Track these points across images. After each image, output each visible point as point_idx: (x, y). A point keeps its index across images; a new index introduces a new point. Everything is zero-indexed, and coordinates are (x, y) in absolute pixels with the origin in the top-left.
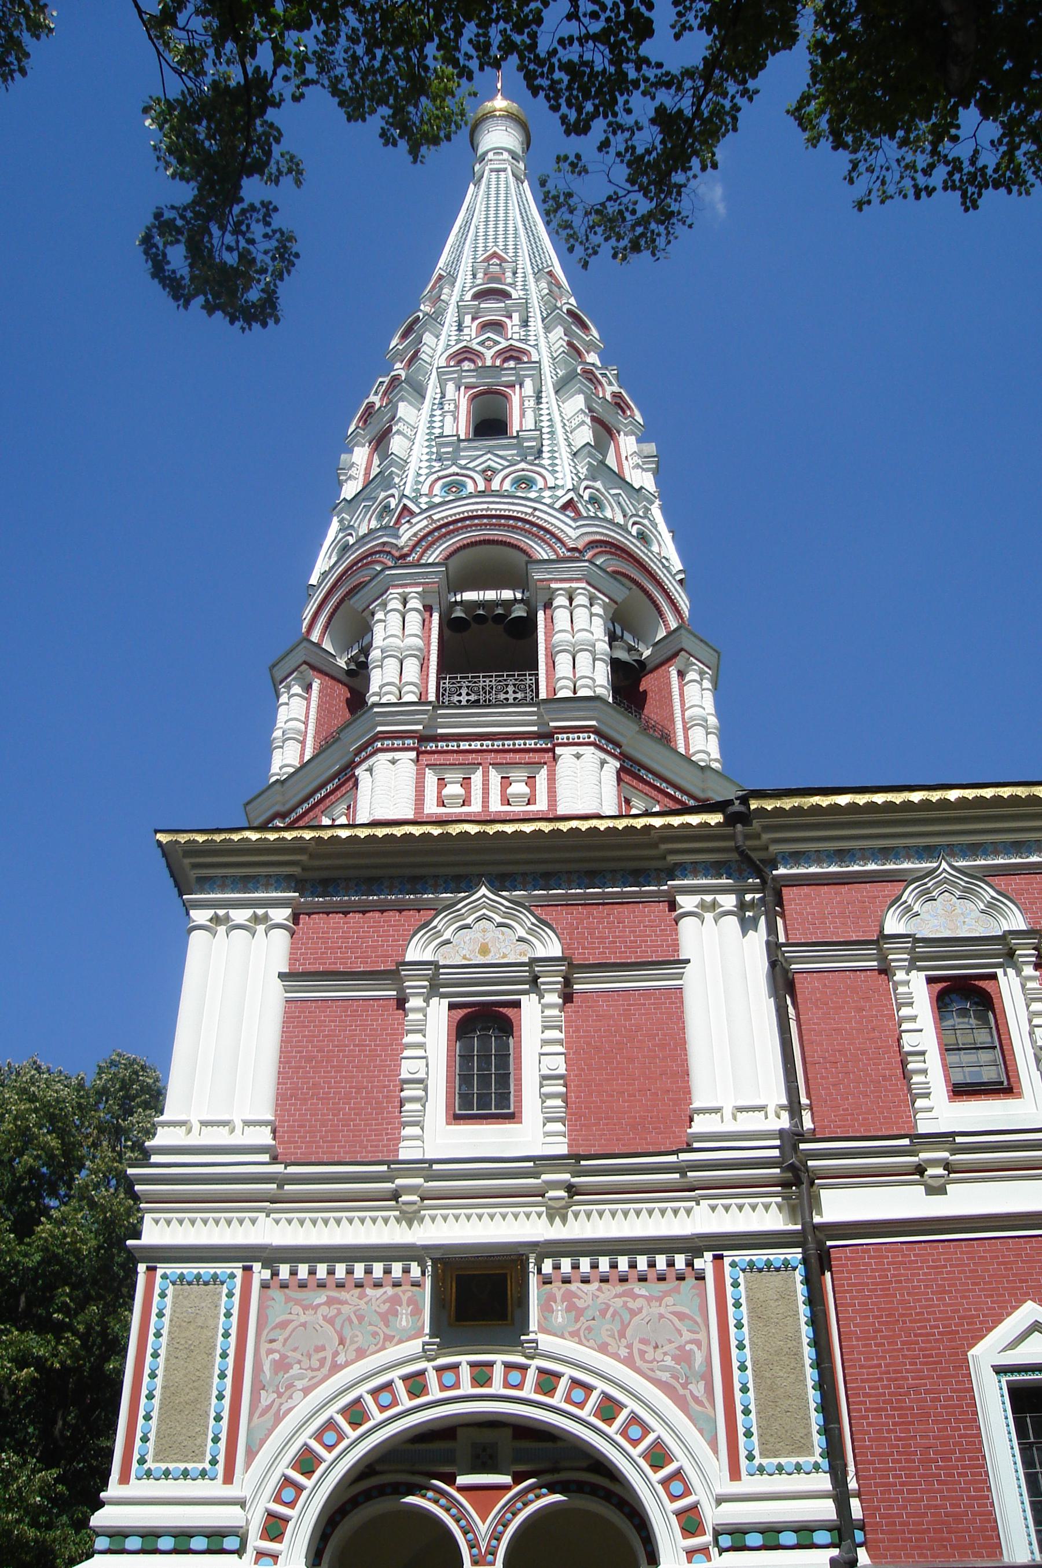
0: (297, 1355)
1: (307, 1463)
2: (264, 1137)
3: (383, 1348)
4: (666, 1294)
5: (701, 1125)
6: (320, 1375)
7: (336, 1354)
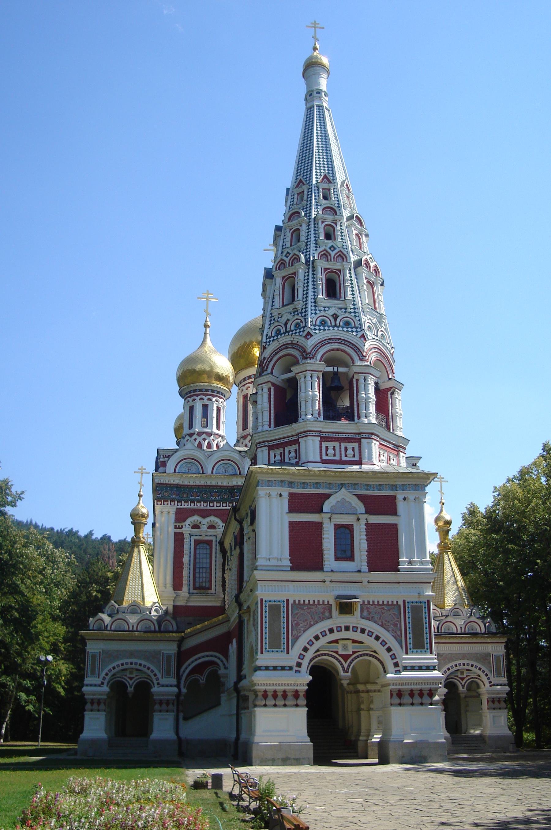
0: (301, 622)
1: (305, 649)
3: (322, 620)
4: (391, 609)
6: (307, 627)
7: (311, 622)
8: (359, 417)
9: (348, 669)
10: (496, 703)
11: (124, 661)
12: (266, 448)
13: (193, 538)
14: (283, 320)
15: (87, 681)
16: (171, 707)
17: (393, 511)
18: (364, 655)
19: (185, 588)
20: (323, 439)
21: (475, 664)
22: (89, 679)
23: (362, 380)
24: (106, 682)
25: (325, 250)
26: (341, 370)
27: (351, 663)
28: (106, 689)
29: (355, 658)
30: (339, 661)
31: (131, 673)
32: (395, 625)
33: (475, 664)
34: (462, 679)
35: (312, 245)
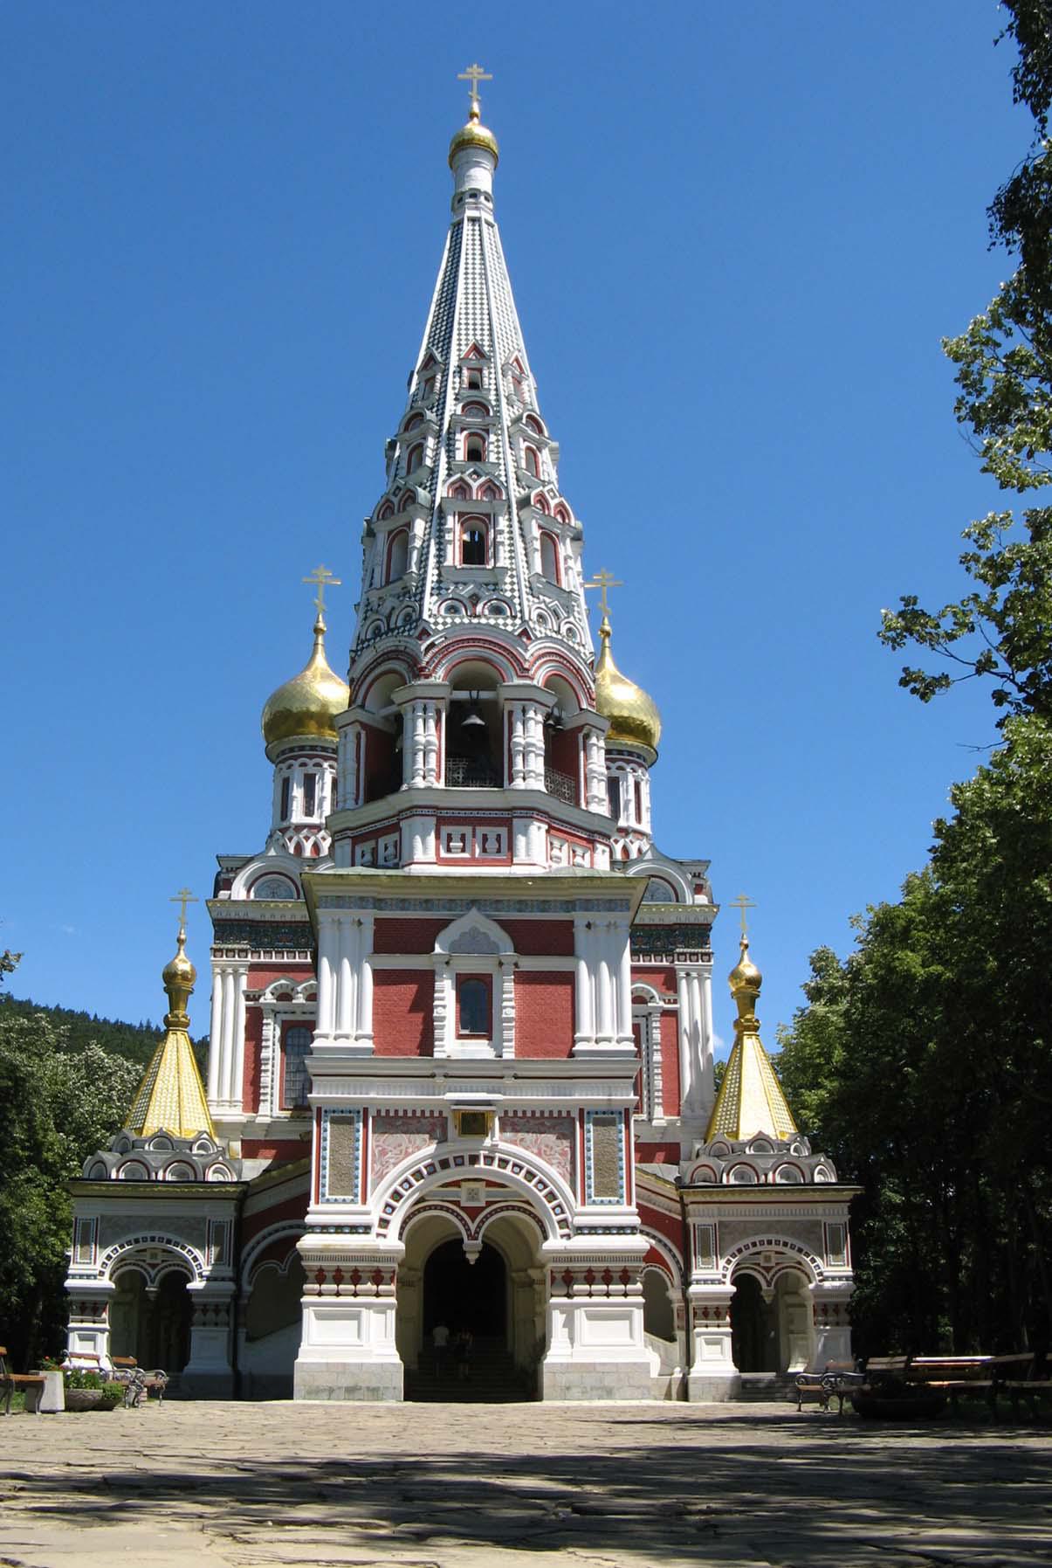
2: (369, 1044)
5: (579, 1047)
8: (511, 780)
9: (477, 1233)
10: (831, 1311)
12: (349, 841)
14: (385, 609)
15: (73, 1268)
16: (223, 1316)
17: (568, 950)
18: (507, 1208)
19: (264, 1108)
20: (441, 821)
21: (790, 1241)
23: (518, 714)
24: (108, 1271)
25: (461, 479)
26: (485, 695)
27: (482, 1222)
29: (491, 1214)
30: (462, 1219)
31: (154, 1256)
32: (563, 1154)
33: (790, 1241)
34: (768, 1269)
35: (443, 472)
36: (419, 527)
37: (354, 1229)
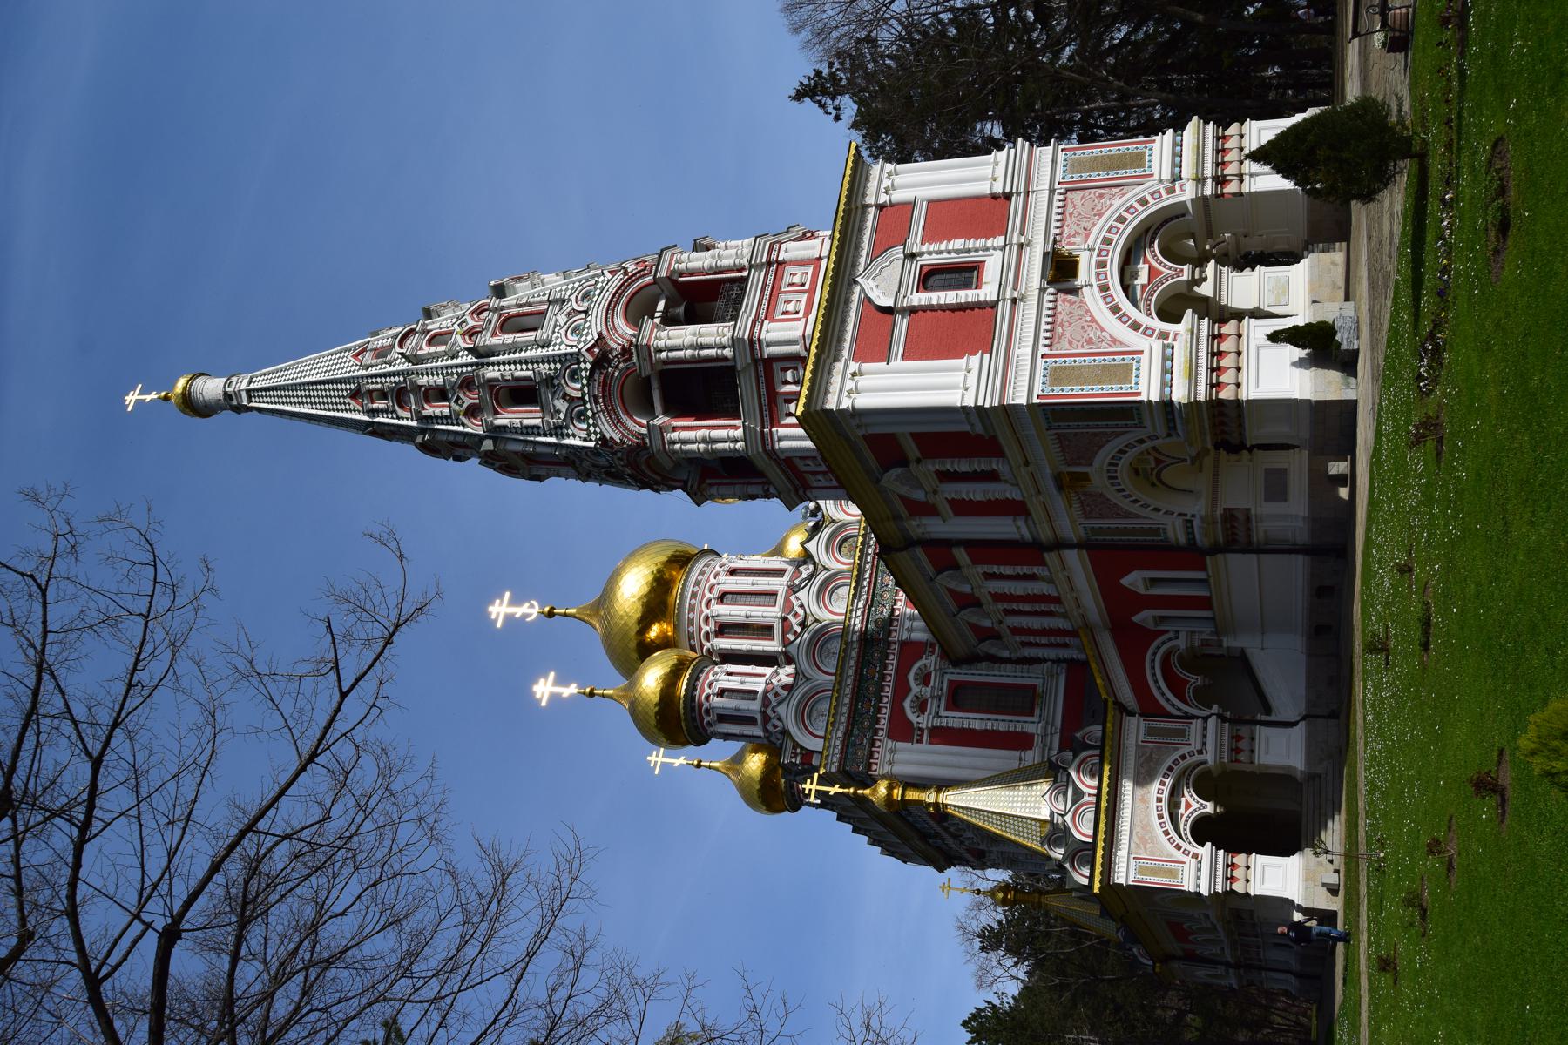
11: (1154, 814)
13: (942, 713)
15: (1189, 886)
19: (1030, 729)
22: (1185, 883)
23: (682, 266)
25: (463, 335)
28: (1205, 850)
32: (1101, 196)
36: (492, 373)
37: (1168, 358)
